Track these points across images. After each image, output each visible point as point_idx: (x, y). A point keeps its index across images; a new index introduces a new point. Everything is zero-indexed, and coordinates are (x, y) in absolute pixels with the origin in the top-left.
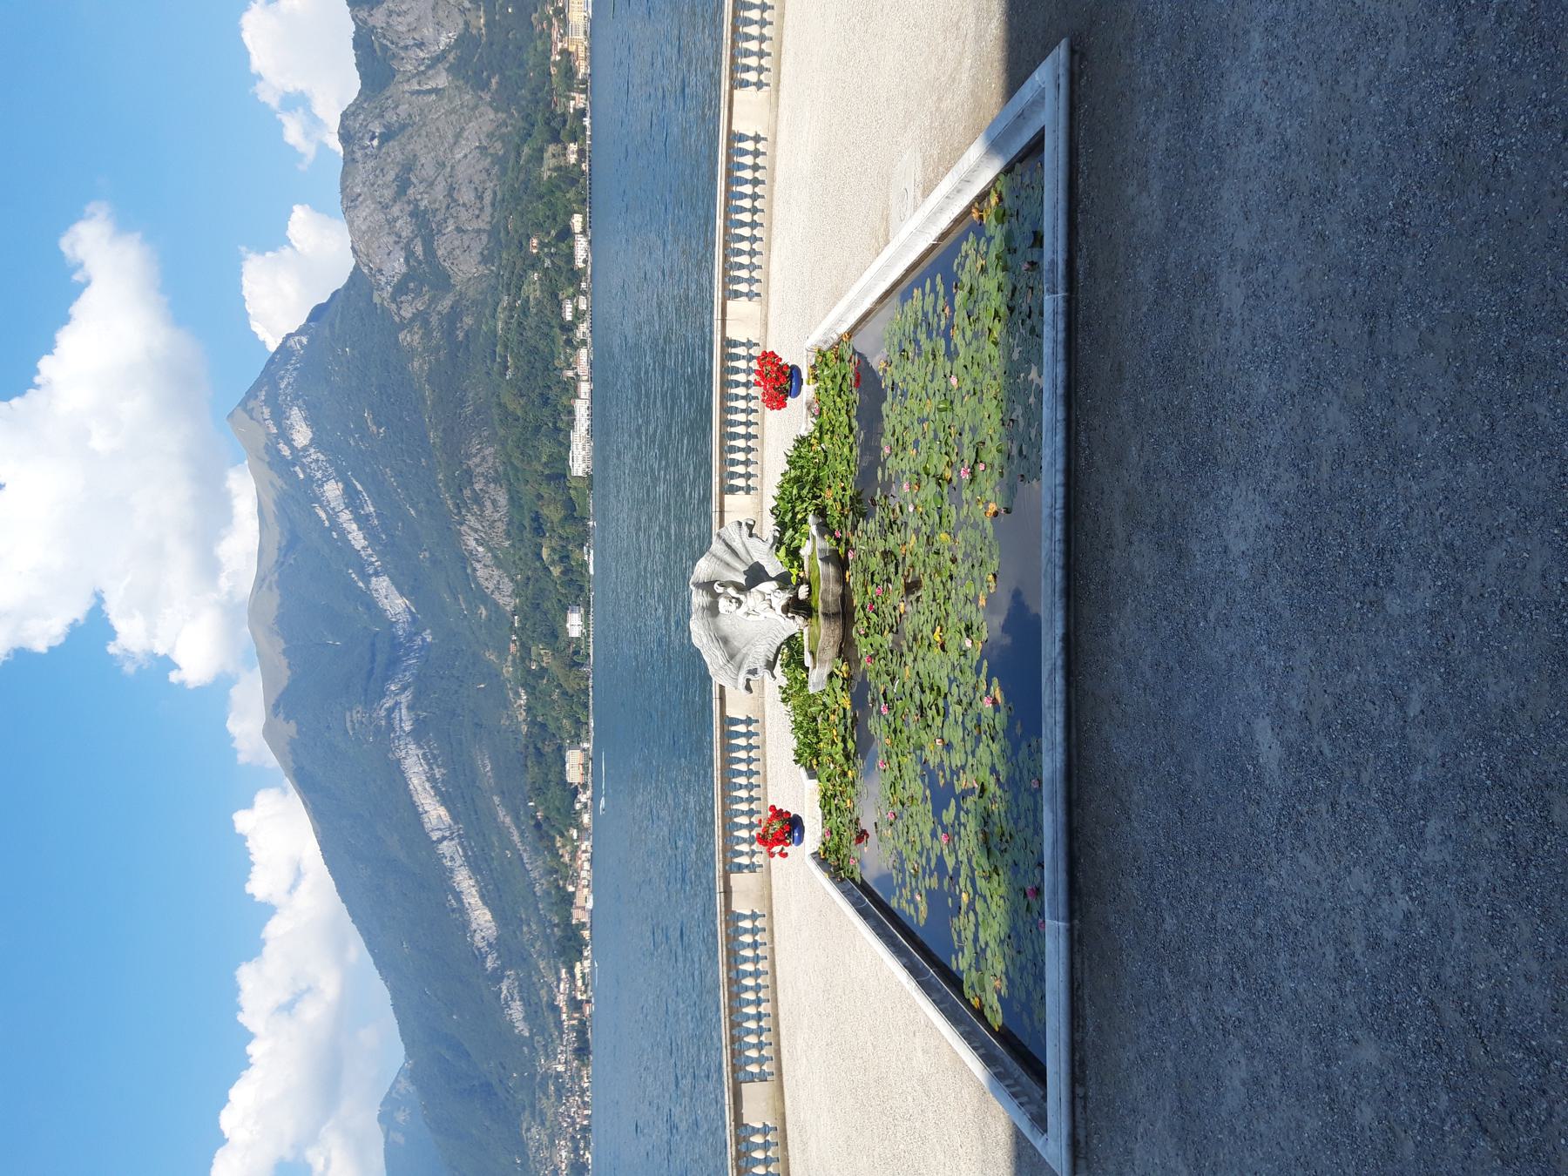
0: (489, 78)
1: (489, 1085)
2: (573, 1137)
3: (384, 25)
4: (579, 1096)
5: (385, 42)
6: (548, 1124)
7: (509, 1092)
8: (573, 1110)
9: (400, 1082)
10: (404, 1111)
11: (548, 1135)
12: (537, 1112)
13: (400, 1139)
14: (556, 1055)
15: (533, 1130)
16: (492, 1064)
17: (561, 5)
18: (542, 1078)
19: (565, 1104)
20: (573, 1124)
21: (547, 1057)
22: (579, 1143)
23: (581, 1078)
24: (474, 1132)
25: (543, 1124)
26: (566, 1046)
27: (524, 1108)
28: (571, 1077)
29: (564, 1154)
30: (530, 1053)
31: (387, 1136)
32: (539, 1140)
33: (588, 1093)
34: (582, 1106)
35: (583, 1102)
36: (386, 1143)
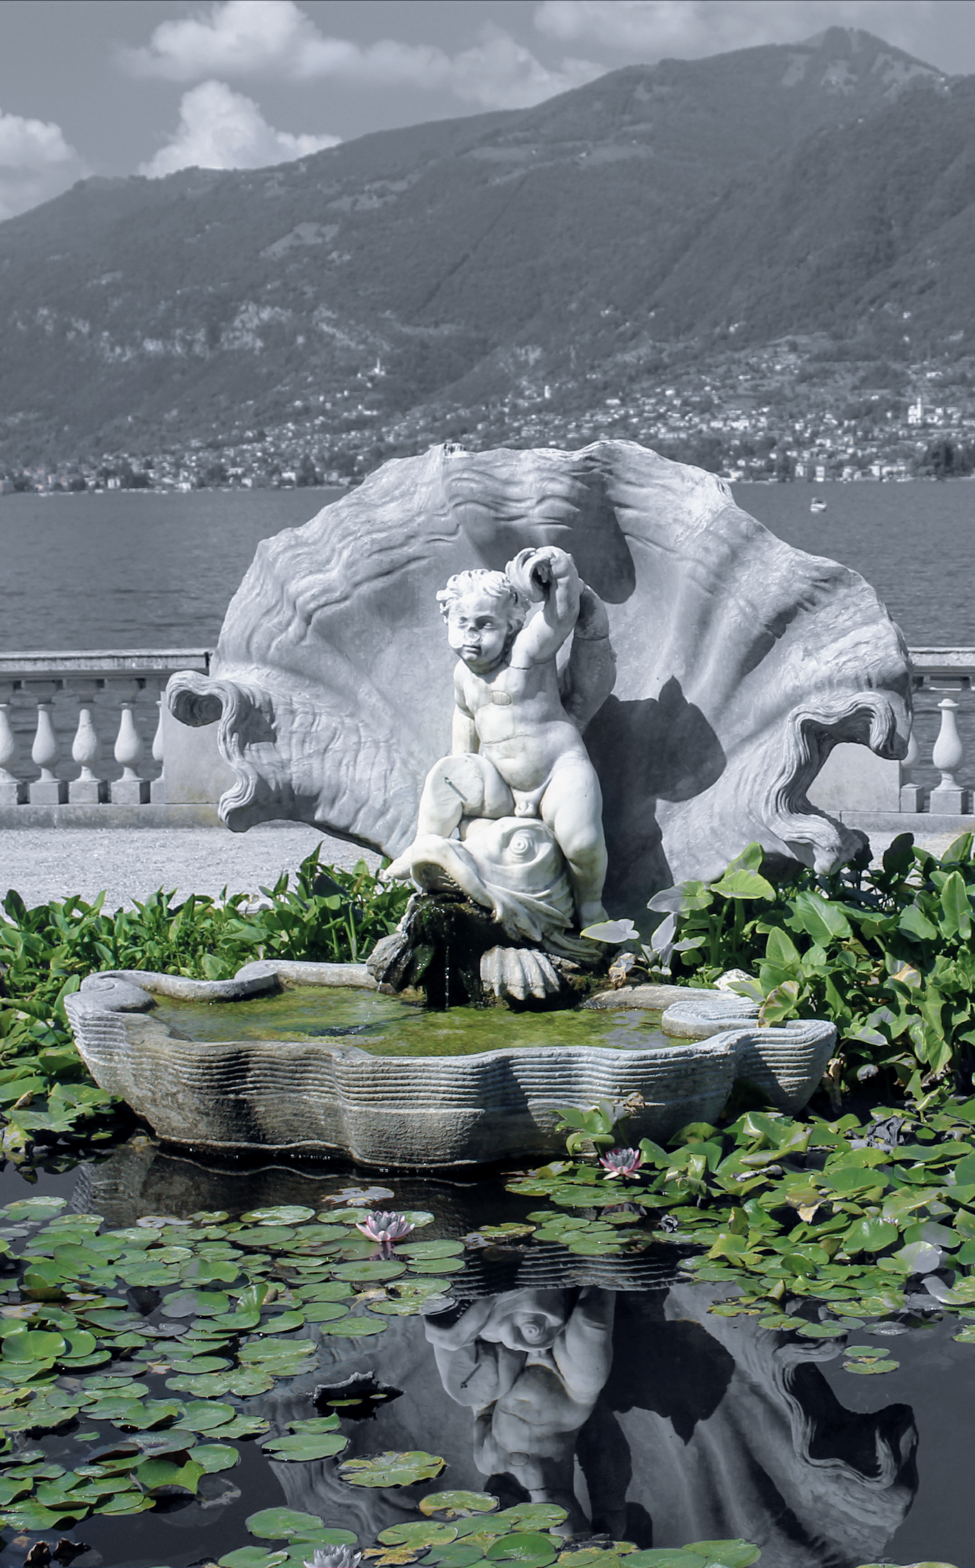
1: (891, 258)
2: (770, 444)
4: (854, 455)
6: (802, 388)
7: (872, 302)
8: (828, 443)
9: (907, 69)
10: (848, 82)
11: (779, 391)
12: (827, 365)
13: (790, 79)
14: (937, 402)
15: (792, 358)
16: (931, 265)
18: (896, 375)
19: (841, 424)
20: (800, 444)
21: (940, 385)
22: (760, 458)
23: (891, 460)
24: (797, 233)
25: (804, 378)
26: (960, 425)
27: (837, 337)
28: (893, 439)
29: (741, 425)
30: (949, 348)
31: (799, 49)
32: (771, 370)
33: (857, 475)
34: (833, 461)
35: (841, 465)
36: (786, 49)
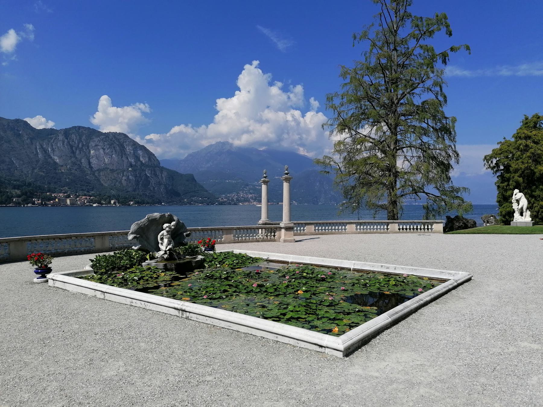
0: (44, 172)
3: (59, 139)
5: (54, 139)
17: (71, 196)
